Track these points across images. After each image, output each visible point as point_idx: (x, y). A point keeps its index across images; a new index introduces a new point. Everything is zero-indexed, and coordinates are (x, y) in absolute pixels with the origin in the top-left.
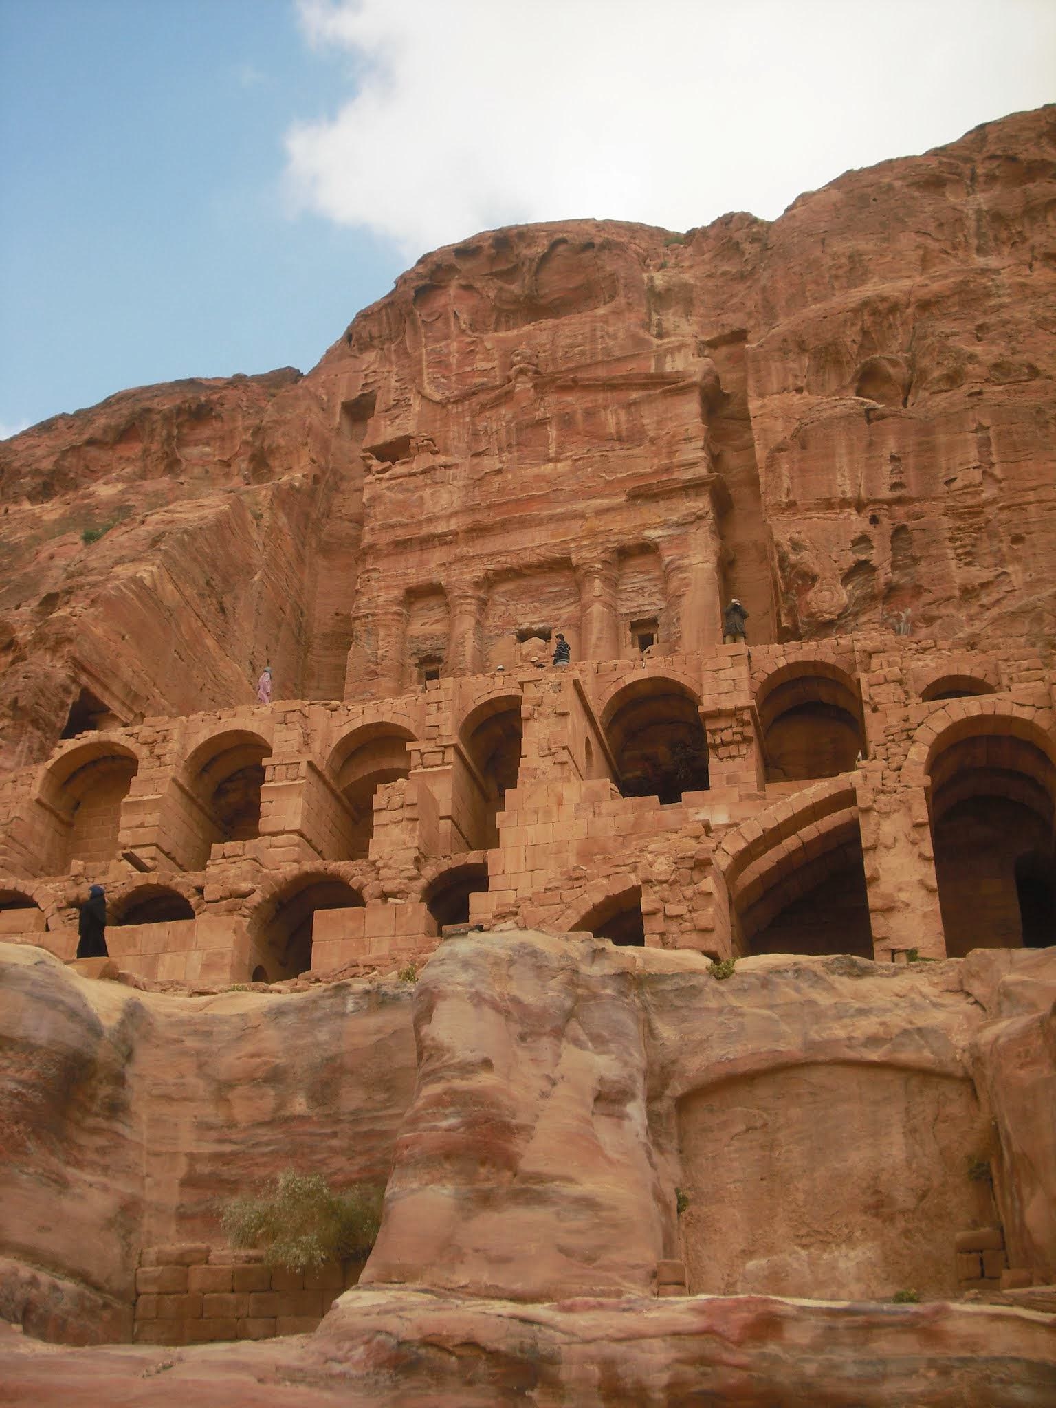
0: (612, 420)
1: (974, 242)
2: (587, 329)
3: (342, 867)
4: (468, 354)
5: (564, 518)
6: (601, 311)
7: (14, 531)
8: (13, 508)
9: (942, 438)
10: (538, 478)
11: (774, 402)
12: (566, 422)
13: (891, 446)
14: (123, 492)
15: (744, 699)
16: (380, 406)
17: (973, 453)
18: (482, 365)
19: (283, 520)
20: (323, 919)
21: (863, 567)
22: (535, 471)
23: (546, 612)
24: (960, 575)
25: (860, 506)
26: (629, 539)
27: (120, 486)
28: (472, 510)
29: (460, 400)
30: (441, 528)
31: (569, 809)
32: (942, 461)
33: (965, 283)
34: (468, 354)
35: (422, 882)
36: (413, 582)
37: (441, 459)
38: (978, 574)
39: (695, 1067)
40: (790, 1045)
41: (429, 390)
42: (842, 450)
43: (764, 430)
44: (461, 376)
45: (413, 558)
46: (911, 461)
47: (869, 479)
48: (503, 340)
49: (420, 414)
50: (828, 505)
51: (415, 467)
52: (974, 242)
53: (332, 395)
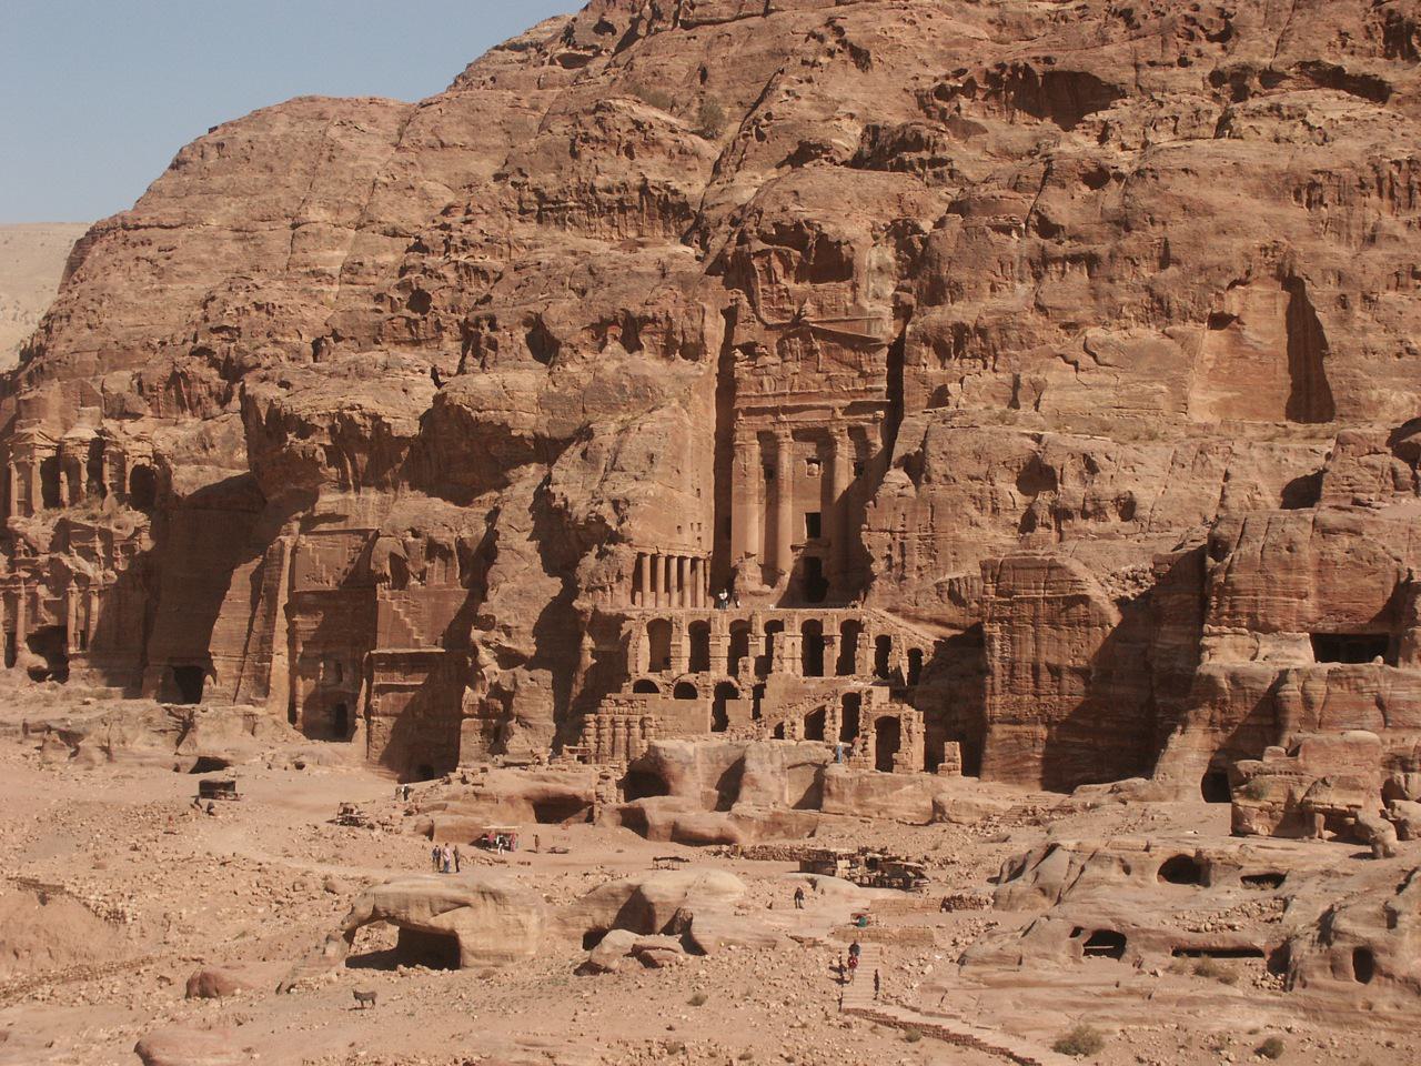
5: (822, 408)
9: (919, 508)
10: (814, 381)
12: (828, 350)
13: (902, 510)
14: (618, 371)
18: (788, 306)
25: (891, 532)
27: (617, 364)
28: (784, 395)
29: (779, 326)
30: (769, 403)
37: (769, 359)
38: (924, 561)
39: (790, 763)
40: (805, 760)
41: (764, 315)
43: (909, 387)
46: (908, 517)
50: (881, 531)
52: (1017, 275)
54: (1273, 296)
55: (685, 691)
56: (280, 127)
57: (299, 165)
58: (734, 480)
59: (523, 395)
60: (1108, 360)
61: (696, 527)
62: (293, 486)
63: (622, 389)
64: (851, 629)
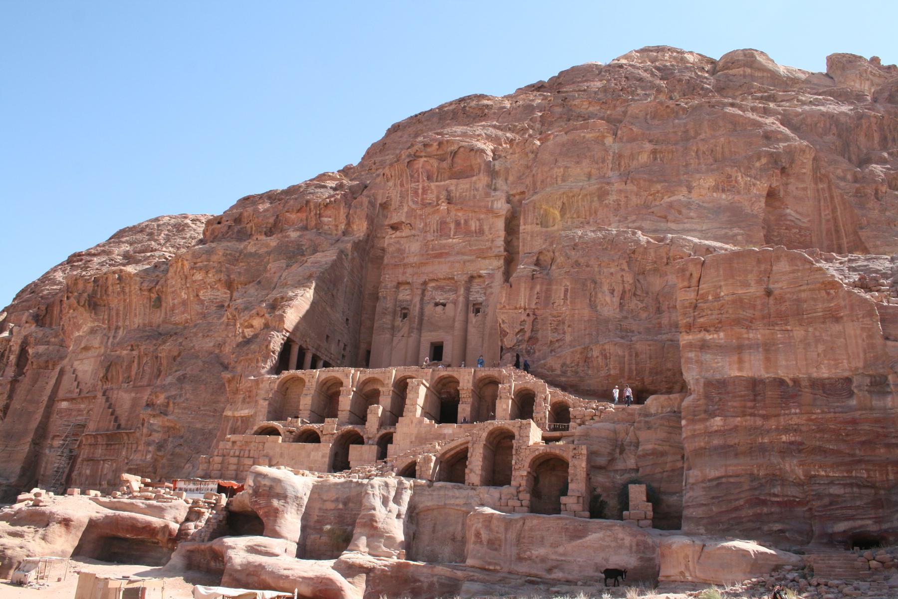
0: (474, 225)
1: (610, 166)
2: (468, 186)
3: (358, 429)
4: (425, 191)
6: (474, 178)
7: (260, 248)
8: (260, 238)
9: (554, 287)
11: (529, 228)
12: (458, 224)
14: (300, 236)
15: (470, 386)
16: (392, 208)
17: (562, 296)
19: (356, 254)
20: (352, 447)
21: (521, 330)
22: (445, 241)
23: (445, 296)
24: (551, 336)
26: (475, 274)
31: (414, 425)
32: (553, 295)
33: (601, 188)
34: (425, 191)
35: (378, 435)
36: (400, 280)
37: (413, 232)
42: (522, 289)
44: (423, 199)
45: (401, 270)
47: (529, 300)
48: (437, 186)
49: (407, 213)
50: (516, 308)
51: (404, 234)
53: (375, 199)
54: (805, 189)
55: (312, 437)
56: (166, 219)
57: (166, 232)
58: (376, 318)
59: (228, 252)
60: (692, 214)
61: (342, 346)
62: (77, 334)
63: (299, 246)
64: (487, 390)
